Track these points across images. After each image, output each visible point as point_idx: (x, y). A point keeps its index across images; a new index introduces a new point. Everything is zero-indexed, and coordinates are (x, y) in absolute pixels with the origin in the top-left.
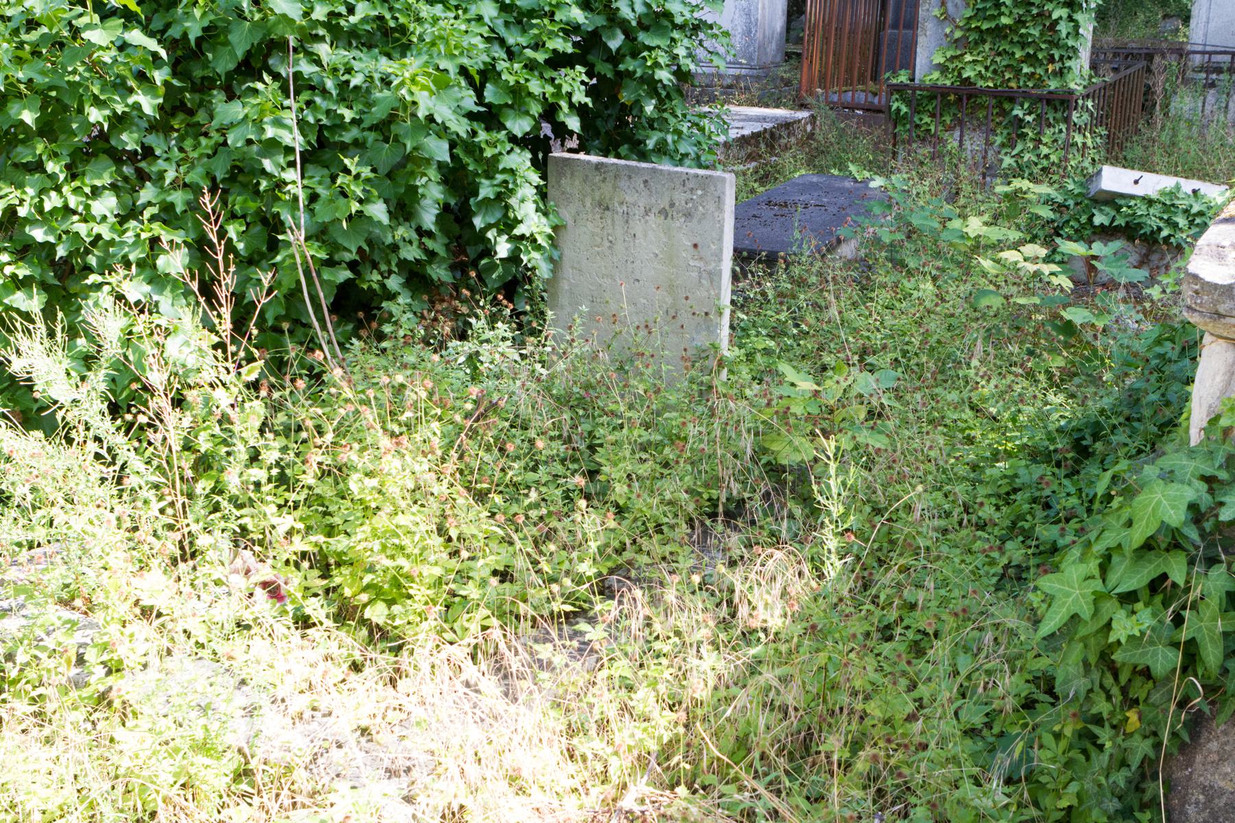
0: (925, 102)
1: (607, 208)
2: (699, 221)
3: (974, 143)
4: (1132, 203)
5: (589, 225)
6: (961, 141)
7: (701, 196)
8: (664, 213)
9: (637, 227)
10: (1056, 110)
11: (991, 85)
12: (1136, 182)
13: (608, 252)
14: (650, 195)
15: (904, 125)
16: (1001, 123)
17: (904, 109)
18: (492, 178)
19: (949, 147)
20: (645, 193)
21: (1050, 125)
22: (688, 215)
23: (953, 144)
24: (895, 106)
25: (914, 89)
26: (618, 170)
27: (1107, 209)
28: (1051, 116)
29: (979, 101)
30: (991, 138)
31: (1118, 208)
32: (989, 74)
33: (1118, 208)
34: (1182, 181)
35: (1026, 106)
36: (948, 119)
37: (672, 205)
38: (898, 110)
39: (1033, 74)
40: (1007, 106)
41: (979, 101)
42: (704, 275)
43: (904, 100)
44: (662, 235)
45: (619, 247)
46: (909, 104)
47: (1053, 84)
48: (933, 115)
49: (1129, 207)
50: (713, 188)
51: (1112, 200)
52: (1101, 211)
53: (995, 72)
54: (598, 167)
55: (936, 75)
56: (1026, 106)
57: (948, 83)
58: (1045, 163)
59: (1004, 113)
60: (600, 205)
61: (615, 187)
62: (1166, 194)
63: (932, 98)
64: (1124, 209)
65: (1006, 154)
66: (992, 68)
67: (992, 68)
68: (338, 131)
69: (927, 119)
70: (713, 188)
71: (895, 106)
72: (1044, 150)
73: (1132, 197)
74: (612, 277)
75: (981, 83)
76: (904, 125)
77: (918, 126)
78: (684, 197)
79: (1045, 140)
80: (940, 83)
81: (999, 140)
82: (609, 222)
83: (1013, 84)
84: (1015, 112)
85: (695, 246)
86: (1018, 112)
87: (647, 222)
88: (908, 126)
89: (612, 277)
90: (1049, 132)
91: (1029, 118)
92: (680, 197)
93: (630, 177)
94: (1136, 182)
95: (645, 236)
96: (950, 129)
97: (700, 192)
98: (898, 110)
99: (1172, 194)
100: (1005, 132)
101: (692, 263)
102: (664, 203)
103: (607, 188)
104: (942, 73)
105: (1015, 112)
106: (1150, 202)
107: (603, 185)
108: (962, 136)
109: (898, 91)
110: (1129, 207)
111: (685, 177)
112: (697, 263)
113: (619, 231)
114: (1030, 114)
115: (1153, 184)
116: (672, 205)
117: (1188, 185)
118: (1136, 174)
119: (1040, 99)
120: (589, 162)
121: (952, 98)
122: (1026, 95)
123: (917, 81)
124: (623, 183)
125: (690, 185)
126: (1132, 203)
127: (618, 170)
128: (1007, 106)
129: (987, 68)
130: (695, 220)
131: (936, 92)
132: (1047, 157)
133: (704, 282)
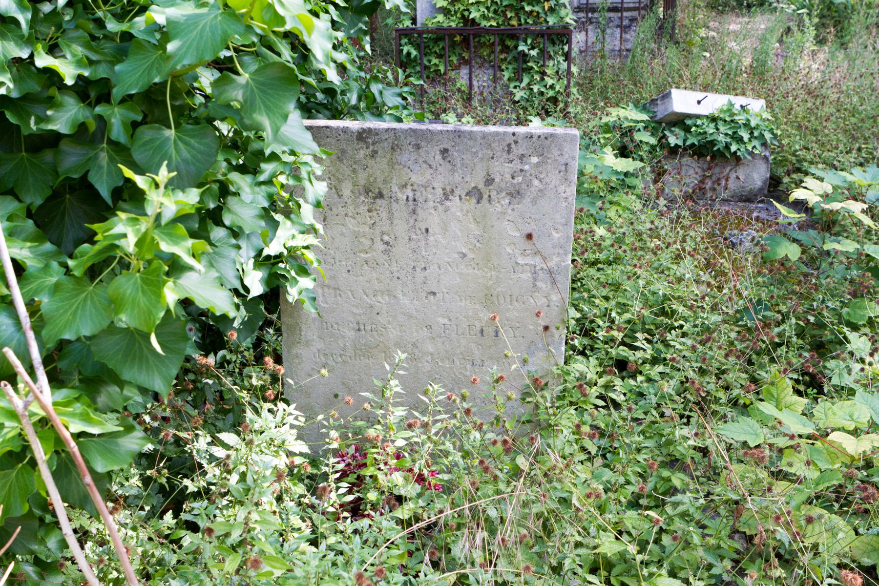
0: (431, 44)
1: (381, 195)
2: (534, 202)
3: (482, 79)
4: (699, 122)
5: (350, 223)
6: (470, 79)
7: (537, 165)
8: (476, 194)
9: (431, 218)
10: (554, 43)
11: (494, 24)
12: (699, 102)
13: (382, 258)
14: (453, 171)
15: (414, 67)
16: (505, 59)
17: (414, 53)
18: (255, 172)
19: (458, 85)
20: (444, 168)
21: (550, 57)
22: (515, 194)
23: (462, 82)
24: (405, 49)
25: (420, 33)
26: (396, 138)
27: (677, 130)
28: (551, 49)
29: (483, 40)
30: (498, 74)
31: (687, 129)
32: (491, 15)
33: (687, 129)
34: (732, 98)
35: (529, 41)
36: (454, 59)
37: (489, 181)
38: (409, 54)
39: (532, 12)
40: (509, 43)
41: (483, 40)
42: (541, 275)
43: (411, 43)
44: (473, 226)
45: (401, 249)
46: (418, 47)
47: (551, 20)
48: (440, 56)
49: (697, 126)
50: (556, 152)
51: (680, 121)
52: (672, 132)
53: (495, 12)
54: (363, 136)
55: (440, 18)
56: (529, 41)
57: (453, 25)
58: (551, 93)
59: (506, 49)
60: (367, 191)
61: (392, 164)
62: (725, 112)
63: (436, 41)
64: (693, 129)
65: (515, 87)
66: (492, 9)
67: (492, 9)
68: (38, 109)
69: (435, 61)
70: (556, 152)
71: (405, 49)
72: (549, 81)
73: (698, 117)
74: (390, 293)
75: (484, 23)
76: (414, 67)
77: (426, 68)
78: (508, 168)
79: (548, 72)
80: (445, 25)
81: (507, 75)
82: (384, 215)
83: (514, 22)
84: (520, 48)
85: (529, 236)
86: (522, 47)
87: (447, 210)
88: (418, 68)
89: (390, 293)
90: (551, 63)
91: (534, 53)
92: (502, 170)
93: (418, 147)
94: (699, 102)
95: (445, 228)
96: (457, 68)
97: (535, 160)
98: (409, 54)
99: (730, 110)
100: (510, 67)
101: (521, 261)
102: (477, 180)
103: (379, 167)
104: (445, 15)
105: (520, 48)
106: (713, 119)
107: (371, 162)
108: (470, 74)
109: (406, 35)
110: (697, 126)
111: (511, 139)
112: (530, 260)
113: (401, 227)
114: (533, 48)
115: (714, 103)
116: (489, 181)
117: (739, 101)
118: (700, 95)
119: (541, 34)
120: (345, 130)
121: (458, 38)
122: (528, 32)
123: (419, 25)
124: (406, 156)
125: (517, 151)
126: (699, 122)
127: (396, 138)
128: (509, 43)
129: (488, 8)
130: (527, 200)
131: (440, 34)
132: (552, 87)
133: (540, 284)
